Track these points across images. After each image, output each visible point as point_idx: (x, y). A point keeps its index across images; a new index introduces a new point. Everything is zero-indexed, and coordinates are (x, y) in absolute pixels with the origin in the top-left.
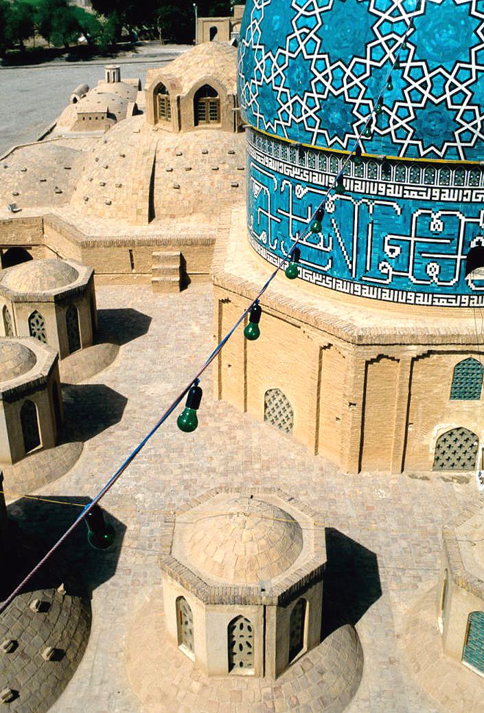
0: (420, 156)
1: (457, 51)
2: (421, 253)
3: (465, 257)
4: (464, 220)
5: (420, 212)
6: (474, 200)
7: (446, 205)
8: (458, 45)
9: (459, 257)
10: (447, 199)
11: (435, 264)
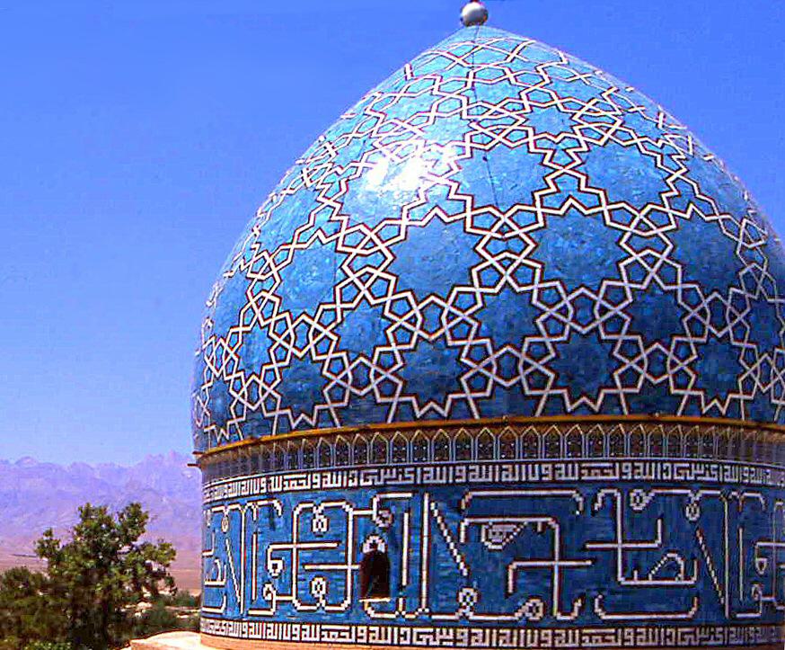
0: (291, 430)
1: (321, 291)
2: (303, 565)
3: (357, 567)
4: (352, 513)
5: (301, 506)
6: (362, 483)
7: (330, 494)
8: (321, 285)
9: (349, 567)
10: (329, 485)
11: (321, 579)
